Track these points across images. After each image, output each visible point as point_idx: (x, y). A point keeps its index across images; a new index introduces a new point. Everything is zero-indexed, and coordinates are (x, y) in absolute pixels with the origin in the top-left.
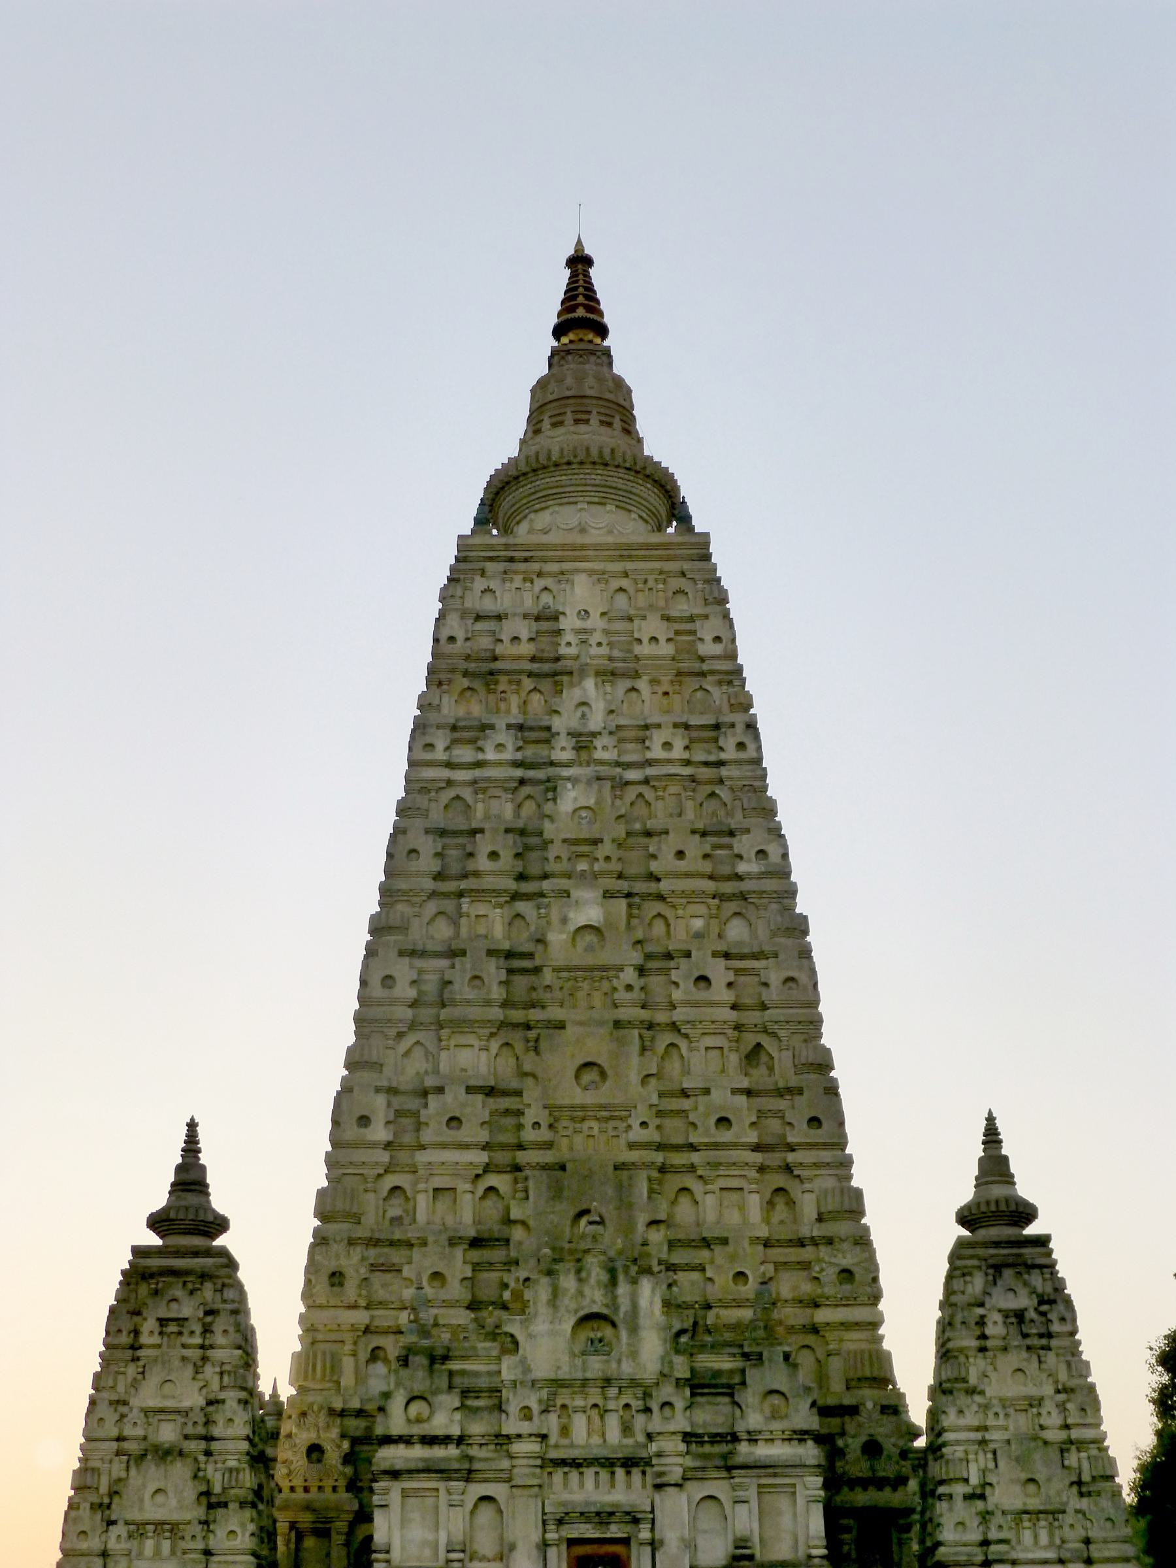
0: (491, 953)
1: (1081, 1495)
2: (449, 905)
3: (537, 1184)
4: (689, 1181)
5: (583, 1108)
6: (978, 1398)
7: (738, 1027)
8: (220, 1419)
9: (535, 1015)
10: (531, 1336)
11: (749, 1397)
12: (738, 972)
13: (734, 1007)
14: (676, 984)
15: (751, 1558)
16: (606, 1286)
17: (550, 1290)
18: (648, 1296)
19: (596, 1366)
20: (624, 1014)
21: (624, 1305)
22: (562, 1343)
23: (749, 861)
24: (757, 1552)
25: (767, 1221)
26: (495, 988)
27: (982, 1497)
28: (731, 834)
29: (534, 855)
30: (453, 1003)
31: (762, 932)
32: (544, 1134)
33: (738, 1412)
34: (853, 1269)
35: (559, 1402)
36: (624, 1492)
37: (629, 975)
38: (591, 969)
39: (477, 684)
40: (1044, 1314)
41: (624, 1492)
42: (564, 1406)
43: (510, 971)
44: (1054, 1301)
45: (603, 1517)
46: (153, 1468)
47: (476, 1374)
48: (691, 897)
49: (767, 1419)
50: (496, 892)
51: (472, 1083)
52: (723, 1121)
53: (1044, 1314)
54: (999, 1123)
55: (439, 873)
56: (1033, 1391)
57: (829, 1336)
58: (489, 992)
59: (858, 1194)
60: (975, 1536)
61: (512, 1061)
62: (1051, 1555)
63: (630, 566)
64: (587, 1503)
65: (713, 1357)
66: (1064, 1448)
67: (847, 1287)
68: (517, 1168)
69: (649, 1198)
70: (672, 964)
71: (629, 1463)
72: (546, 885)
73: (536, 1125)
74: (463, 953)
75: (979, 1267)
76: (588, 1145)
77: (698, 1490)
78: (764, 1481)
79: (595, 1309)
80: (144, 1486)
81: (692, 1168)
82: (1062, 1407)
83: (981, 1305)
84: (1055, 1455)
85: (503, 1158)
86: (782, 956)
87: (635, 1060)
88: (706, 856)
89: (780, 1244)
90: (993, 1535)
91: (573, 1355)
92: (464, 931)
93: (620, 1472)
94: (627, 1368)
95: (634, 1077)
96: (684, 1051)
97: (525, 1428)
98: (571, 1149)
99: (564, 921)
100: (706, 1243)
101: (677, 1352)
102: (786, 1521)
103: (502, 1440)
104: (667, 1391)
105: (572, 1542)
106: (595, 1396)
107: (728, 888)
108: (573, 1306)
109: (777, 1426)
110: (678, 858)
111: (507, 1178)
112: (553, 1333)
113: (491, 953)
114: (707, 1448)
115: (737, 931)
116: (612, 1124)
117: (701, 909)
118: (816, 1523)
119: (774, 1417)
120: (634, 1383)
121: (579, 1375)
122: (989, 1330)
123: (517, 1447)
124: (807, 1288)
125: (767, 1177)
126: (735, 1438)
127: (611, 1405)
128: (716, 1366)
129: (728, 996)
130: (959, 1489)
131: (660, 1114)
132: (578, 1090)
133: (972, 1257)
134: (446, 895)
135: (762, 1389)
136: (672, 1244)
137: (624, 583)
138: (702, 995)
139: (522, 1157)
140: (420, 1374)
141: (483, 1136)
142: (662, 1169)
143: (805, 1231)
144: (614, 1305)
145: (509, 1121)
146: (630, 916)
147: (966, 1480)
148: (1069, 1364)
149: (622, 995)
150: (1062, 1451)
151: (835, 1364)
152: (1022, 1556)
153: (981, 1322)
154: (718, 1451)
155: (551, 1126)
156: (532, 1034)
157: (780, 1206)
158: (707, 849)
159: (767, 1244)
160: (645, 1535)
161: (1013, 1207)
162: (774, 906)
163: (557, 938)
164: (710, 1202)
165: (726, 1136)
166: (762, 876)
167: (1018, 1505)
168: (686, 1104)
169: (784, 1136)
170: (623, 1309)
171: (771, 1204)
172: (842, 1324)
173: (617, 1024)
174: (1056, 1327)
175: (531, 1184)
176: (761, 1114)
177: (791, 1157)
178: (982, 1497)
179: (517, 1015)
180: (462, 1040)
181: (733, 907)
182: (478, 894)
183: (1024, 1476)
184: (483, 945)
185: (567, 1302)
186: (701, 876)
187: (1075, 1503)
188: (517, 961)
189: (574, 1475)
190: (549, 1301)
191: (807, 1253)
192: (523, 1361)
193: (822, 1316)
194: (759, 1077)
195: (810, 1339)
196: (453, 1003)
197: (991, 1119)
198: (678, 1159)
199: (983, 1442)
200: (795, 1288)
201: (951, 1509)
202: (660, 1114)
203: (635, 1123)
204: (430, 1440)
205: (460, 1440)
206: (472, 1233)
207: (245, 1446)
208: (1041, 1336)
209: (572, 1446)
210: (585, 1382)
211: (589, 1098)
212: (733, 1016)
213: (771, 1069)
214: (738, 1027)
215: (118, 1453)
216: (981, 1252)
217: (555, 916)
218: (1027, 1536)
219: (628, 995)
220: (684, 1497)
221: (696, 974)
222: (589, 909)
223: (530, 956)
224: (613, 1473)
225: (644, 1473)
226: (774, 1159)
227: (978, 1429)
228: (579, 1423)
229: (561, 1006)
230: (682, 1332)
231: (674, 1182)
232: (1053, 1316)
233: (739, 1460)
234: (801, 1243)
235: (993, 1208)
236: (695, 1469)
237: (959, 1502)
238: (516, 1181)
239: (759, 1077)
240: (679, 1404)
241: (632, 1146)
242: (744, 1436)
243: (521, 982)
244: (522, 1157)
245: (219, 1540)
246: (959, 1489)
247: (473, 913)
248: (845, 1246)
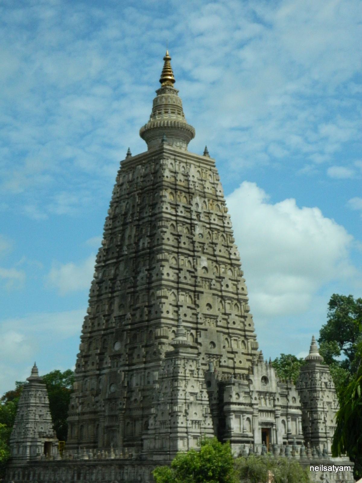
2: (176, 255)
8: (203, 395)
10: (255, 380)
36: (270, 419)
38: (205, 278)
39: (173, 192)
45: (267, 424)
48: (224, 263)
59: (257, 343)
63: (201, 165)
71: (271, 412)
94: (270, 390)
103: (251, 405)
104: (277, 396)
110: (221, 251)
112: (258, 380)
123: (255, 407)
137: (199, 169)
140: (237, 388)
143: (250, 352)
144: (267, 374)
160: (274, 428)
163: (199, 268)
165: (234, 326)
173: (214, 294)
175: (202, 334)
182: (183, 254)
185: (260, 373)
199: (324, 411)
204: (239, 404)
207: (208, 403)
215: (185, 403)
222: (204, 262)
223: (193, 272)
235: (315, 358)
238: (197, 332)
245: (207, 426)
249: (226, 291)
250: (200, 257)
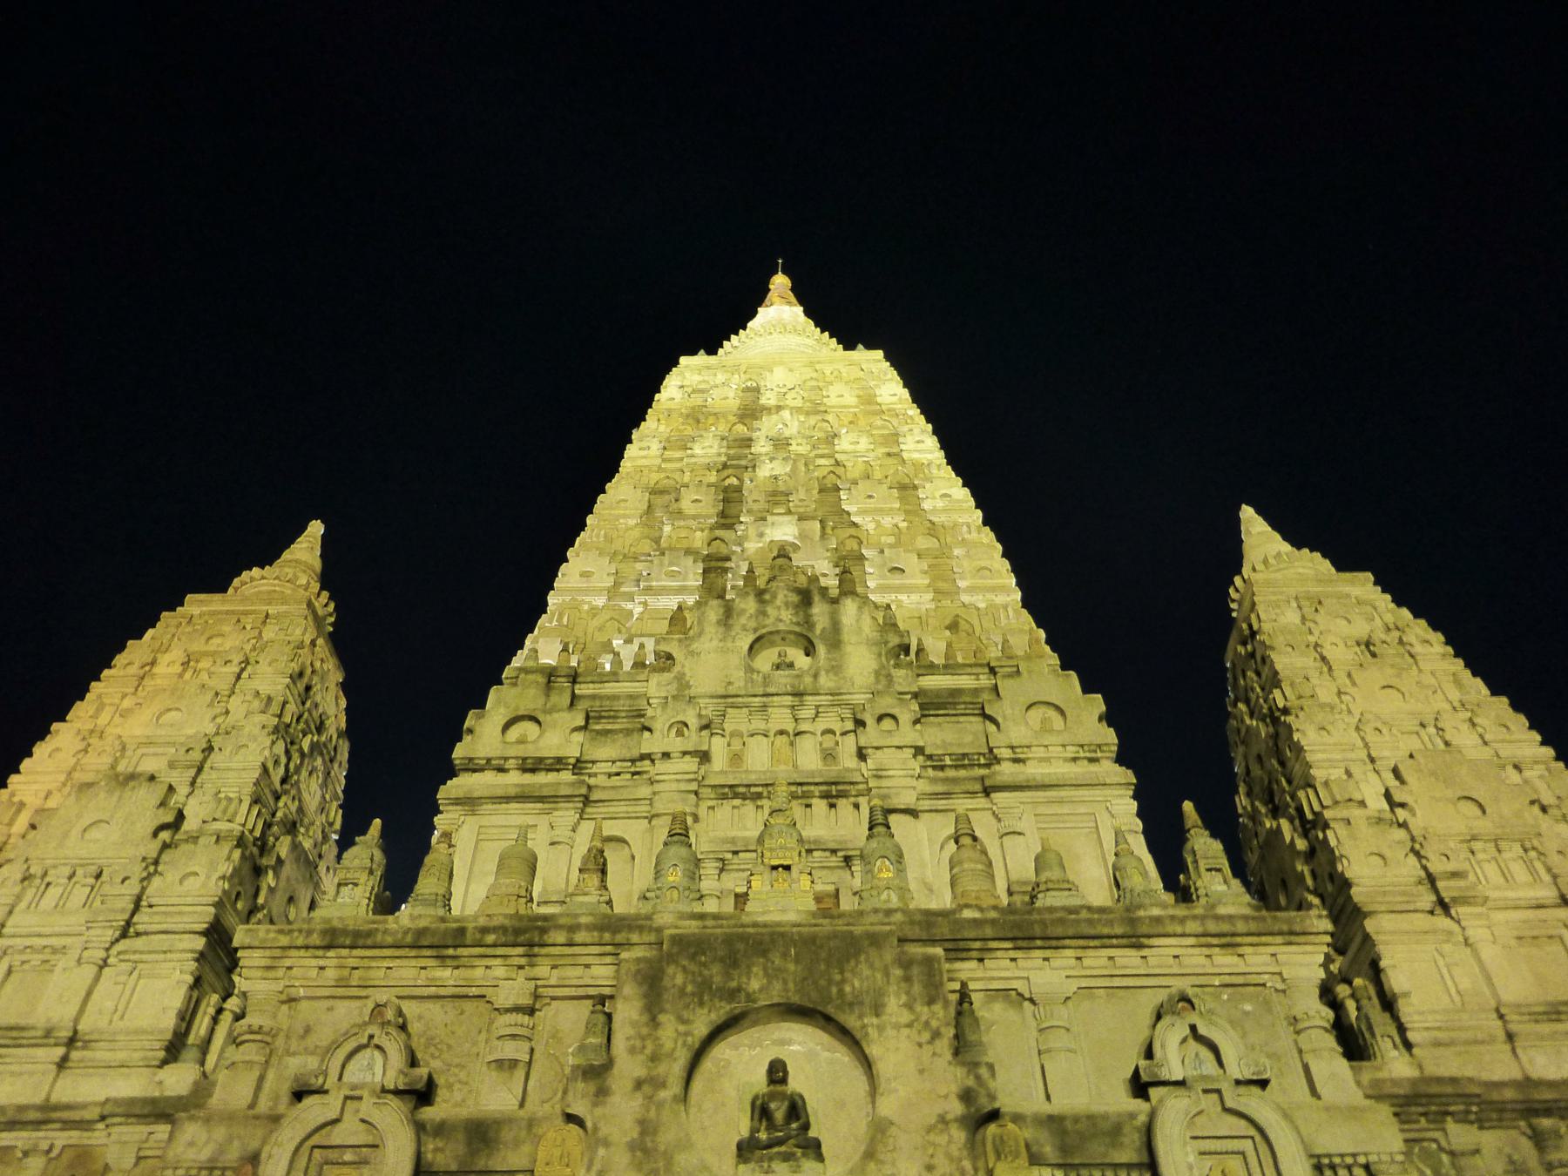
16: (796, 607)
17: (722, 610)
33: (992, 728)
46: (102, 795)
47: (615, 697)
80: (79, 816)
97: (675, 744)
99: (761, 535)
106: (780, 717)
108: (752, 624)
114: (951, 773)
138: (896, 580)
190: (719, 622)
192: (680, 678)
205: (579, 766)
225: (856, 806)
242: (1005, 753)
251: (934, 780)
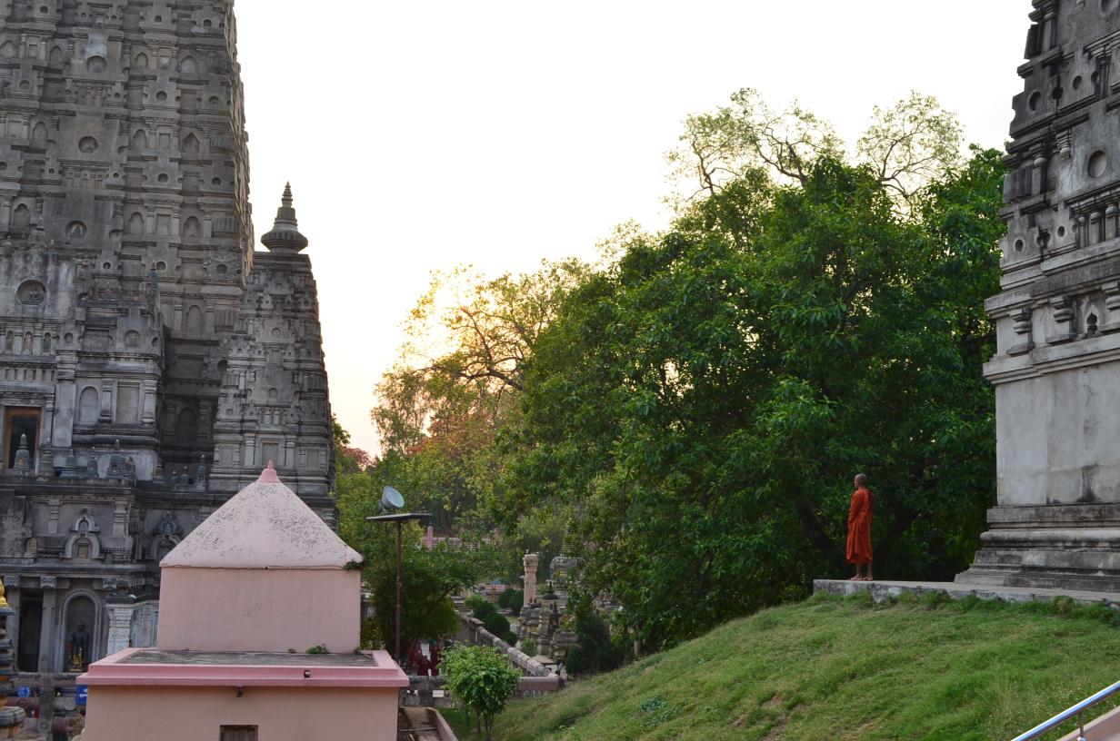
0: (35, 68)
1: (301, 399)
2: (14, 37)
3: (48, 203)
4: (140, 210)
5: (81, 162)
6: (251, 343)
7: (180, 123)
9: (59, 106)
11: (119, 334)
12: (183, 91)
13: (180, 111)
14: (146, 95)
15: (110, 422)
18: (66, 273)
19: (30, 309)
20: (111, 110)
21: (51, 276)
22: (11, 296)
23: (200, 26)
24: (114, 420)
25: (182, 235)
26: (36, 89)
27: (245, 396)
28: (192, 9)
29: (70, 12)
30: (10, 96)
31: (202, 69)
32: (56, 176)
34: (228, 265)
35: (7, 330)
36: (38, 383)
37: (118, 88)
38: (97, 82)
40: (295, 299)
41: (38, 383)
42: (10, 332)
43: (47, 80)
44: (309, 289)
45: (26, 394)
49: (127, 346)
50: (42, 32)
51: (15, 143)
52: (163, 177)
53: (295, 299)
54: (292, 189)
55: (10, 17)
56: (283, 341)
57: (208, 301)
58: (32, 91)
60: (238, 417)
61: (44, 133)
62: (278, 430)
64: (18, 387)
65: (100, 310)
66: (296, 372)
67: (222, 275)
68: (38, 194)
69: (114, 217)
70: (146, 83)
72: (74, 30)
73: (51, 171)
74: (18, 66)
75: (264, 270)
76: (81, 184)
77: (83, 384)
78: (121, 380)
79: (33, 278)
81: (142, 202)
82: (297, 351)
83: (262, 291)
84: (288, 375)
85: (29, 188)
86: (210, 84)
87: (115, 138)
88: (174, 21)
89: (188, 248)
90: (246, 418)
91: (17, 304)
92: (21, 54)
93: (39, 372)
94: (48, 313)
95: (114, 148)
96: (147, 134)
98: (72, 186)
99: (83, 52)
100: (144, 245)
101: (79, 306)
102: (133, 403)
104: (70, 327)
105: (8, 408)
107: (185, 41)
108: (20, 276)
109: (131, 350)
111: (32, 199)
113: (35, 68)
114: (92, 361)
115: (188, 67)
116: (98, 173)
117: (168, 52)
118: (150, 405)
119: (131, 346)
120: (52, 322)
121: (20, 315)
122: (263, 306)
124: (200, 273)
125: (186, 210)
126: (108, 357)
127: (38, 333)
128: (102, 314)
129: (175, 105)
130: (233, 391)
131: (127, 169)
132: (79, 152)
133: (261, 264)
134: (13, 31)
135: (125, 329)
136: (124, 244)
138: (160, 103)
139: (41, 188)
141: (19, 175)
142: (125, 201)
144: (45, 277)
145: (37, 168)
146: (123, 53)
147: (237, 387)
148: (306, 327)
149: (112, 99)
150: (293, 374)
151: (210, 317)
152: (262, 429)
153: (259, 301)
154: (95, 364)
155: (60, 172)
156: (56, 118)
157: (192, 226)
158: (175, 16)
159: (180, 247)
160: (49, 406)
161: (289, 238)
162: (212, 54)
163: (78, 62)
164: (149, 221)
165: (164, 185)
166: (205, 35)
167: (264, 401)
168: (143, 165)
169: (197, 187)
170: (49, 279)
171: (186, 225)
172: (217, 295)
173: (107, 116)
174: (302, 307)
175: (44, 204)
176: (186, 174)
177: (200, 200)
178: (245, 396)
179: (48, 106)
180: (14, 118)
181: (186, 52)
183: (269, 386)
184: (31, 63)
186: (170, 32)
187: (296, 402)
188: (51, 74)
189: (12, 372)
191: (202, 255)
193: (206, 290)
194: (190, 153)
195: (198, 303)
196: (10, 96)
197: (288, 187)
198: (135, 196)
199: (250, 367)
200: (193, 273)
201: (225, 402)
202: (127, 169)
203: (111, 175)
206: (7, 230)
208: (293, 311)
209: (12, 355)
210: (23, 320)
211: (86, 157)
212: (176, 116)
213: (198, 148)
214: (180, 123)
216: (266, 261)
217: (77, 49)
218: (267, 419)
219: (116, 99)
220: (74, 387)
221: (158, 90)
223: (60, 71)
224: (35, 371)
226: (189, 200)
227: (249, 359)
228: (18, 342)
229: (76, 103)
230: (85, 294)
231: (132, 209)
232: (302, 301)
233: (108, 368)
234: (200, 248)
235: (283, 237)
236: (82, 371)
237: (231, 399)
239: (190, 153)
240: (76, 335)
241: (109, 187)
243: (53, 86)
244: (41, 188)
246: (233, 391)
247: (28, 44)
248: (224, 252)
249: (153, 107)
250: (86, 36)
251: (83, 364)
